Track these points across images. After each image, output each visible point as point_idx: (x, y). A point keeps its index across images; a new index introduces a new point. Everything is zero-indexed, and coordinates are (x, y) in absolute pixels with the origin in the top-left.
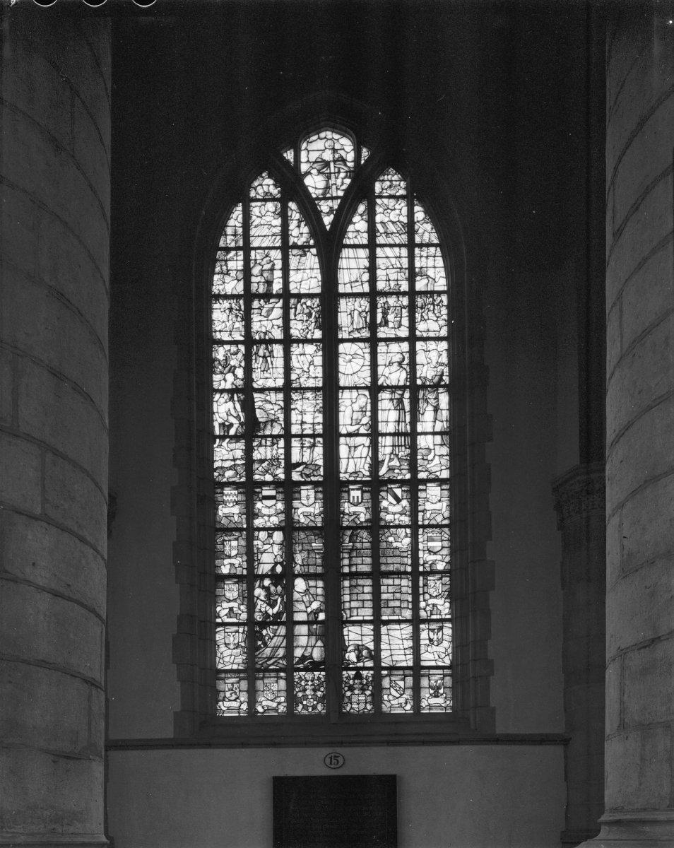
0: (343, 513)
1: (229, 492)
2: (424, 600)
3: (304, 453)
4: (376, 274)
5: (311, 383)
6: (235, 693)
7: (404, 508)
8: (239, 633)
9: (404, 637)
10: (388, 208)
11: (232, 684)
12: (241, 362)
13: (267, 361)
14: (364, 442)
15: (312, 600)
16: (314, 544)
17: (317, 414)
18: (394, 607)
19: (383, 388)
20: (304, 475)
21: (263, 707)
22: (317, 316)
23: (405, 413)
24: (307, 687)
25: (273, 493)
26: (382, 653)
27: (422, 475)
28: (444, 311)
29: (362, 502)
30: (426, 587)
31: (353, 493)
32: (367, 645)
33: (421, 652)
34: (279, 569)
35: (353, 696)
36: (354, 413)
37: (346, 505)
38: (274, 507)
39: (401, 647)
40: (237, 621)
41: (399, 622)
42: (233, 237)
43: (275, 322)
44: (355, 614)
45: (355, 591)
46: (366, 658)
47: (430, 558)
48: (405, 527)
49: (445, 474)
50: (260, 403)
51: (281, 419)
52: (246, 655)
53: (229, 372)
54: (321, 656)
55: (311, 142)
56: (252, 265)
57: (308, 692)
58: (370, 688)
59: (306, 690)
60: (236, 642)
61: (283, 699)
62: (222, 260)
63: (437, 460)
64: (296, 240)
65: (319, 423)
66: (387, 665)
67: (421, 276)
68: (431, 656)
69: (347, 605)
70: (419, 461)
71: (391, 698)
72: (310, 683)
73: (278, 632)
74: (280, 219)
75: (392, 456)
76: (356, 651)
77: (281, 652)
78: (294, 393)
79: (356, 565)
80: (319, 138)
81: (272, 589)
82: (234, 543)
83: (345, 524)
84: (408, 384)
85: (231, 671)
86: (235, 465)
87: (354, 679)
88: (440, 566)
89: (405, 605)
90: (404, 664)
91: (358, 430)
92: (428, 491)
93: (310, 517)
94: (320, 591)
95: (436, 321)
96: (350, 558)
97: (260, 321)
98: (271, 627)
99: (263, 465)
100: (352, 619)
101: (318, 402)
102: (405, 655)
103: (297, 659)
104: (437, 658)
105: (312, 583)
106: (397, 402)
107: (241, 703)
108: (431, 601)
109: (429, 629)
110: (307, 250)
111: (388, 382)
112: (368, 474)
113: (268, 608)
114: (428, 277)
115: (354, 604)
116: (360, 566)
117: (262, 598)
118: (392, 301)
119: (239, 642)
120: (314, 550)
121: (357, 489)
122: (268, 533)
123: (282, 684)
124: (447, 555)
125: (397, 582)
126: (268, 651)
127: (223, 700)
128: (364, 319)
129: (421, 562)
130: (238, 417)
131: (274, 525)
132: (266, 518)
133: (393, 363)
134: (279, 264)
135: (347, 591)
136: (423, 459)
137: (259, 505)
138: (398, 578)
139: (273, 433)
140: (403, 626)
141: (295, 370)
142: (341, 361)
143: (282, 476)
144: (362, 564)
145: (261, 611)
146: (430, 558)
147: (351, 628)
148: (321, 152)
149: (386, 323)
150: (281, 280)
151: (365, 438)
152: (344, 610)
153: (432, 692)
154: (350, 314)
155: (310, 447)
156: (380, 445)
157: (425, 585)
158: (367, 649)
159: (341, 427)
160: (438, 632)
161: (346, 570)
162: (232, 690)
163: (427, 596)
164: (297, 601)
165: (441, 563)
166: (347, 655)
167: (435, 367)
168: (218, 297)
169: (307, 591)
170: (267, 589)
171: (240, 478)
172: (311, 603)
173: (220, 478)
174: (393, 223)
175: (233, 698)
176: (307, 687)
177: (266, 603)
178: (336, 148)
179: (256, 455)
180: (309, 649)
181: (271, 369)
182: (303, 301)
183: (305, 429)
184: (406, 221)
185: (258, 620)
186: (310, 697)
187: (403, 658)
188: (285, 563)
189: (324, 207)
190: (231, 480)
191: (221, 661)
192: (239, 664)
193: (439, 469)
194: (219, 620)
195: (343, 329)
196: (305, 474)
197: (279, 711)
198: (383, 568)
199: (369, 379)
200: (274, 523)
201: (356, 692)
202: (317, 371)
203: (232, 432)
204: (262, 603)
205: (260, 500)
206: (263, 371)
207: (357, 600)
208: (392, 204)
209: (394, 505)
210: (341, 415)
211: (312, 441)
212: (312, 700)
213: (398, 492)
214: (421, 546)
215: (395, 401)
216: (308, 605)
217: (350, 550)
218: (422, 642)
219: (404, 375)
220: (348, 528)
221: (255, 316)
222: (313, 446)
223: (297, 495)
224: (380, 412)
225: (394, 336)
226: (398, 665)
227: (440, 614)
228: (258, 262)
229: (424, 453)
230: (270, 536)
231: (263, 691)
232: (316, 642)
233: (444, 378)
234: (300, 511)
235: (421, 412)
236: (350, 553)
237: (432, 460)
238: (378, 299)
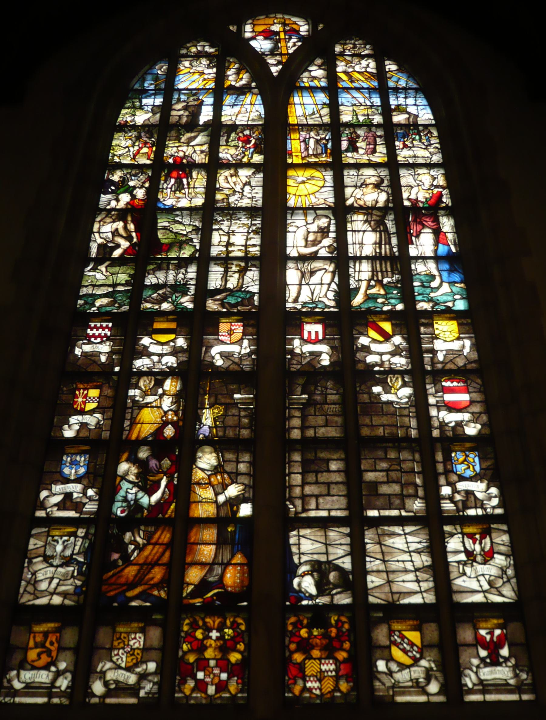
0: (292, 352)
1: (98, 325)
2: (449, 484)
3: (228, 278)
4: (338, 109)
5: (245, 203)
6: (49, 652)
7: (397, 347)
8: (76, 536)
9: (413, 547)
10: (352, 63)
11: (46, 634)
12: (144, 183)
13: (182, 182)
14: (326, 267)
15: (228, 481)
16: (237, 396)
17: (251, 235)
18: (389, 495)
19: (354, 210)
20: (227, 305)
21: (106, 684)
22: (258, 142)
23: (389, 234)
24: (208, 642)
25: (173, 326)
26: (369, 578)
27: (423, 306)
28: (434, 141)
29: (324, 338)
30: (449, 463)
31: (308, 328)
32: (338, 562)
33: (452, 576)
34: (169, 432)
35: (308, 663)
36: (311, 234)
37: (297, 342)
38: (172, 344)
39: (409, 566)
40: (77, 515)
41: (400, 521)
42: (153, 82)
43: (198, 148)
44: (313, 505)
45: (314, 467)
46: (336, 587)
47: (451, 418)
48: (402, 373)
49: (461, 305)
50: (166, 224)
51: (195, 240)
52: (83, 578)
53: (125, 192)
54: (242, 581)
55: (258, 20)
56: (173, 102)
57: (209, 653)
58: (347, 645)
59: (205, 648)
60: (68, 553)
61: (152, 666)
62: (136, 98)
63: (446, 288)
64: (233, 83)
65: (254, 246)
66: (379, 601)
67: (399, 111)
68: (474, 585)
69: (297, 491)
70: (416, 289)
71: (394, 667)
72: (214, 634)
73: (157, 536)
74: (215, 70)
75: (373, 283)
76: (315, 574)
77: (157, 574)
78: (217, 214)
79: (315, 427)
80: (267, 17)
81: (153, 463)
82: (94, 393)
83: (295, 367)
84: (391, 205)
85: (49, 607)
86: (114, 292)
87: (310, 627)
88: (472, 430)
89: (411, 491)
90: (417, 599)
91: (317, 252)
92: (436, 326)
93: (232, 358)
94: (242, 467)
95: (424, 149)
96: (304, 418)
97: (177, 147)
98: (142, 528)
99: (160, 292)
100: (304, 515)
101: (253, 222)
102: (418, 581)
103: (191, 588)
104: (486, 586)
105: (229, 456)
106: (375, 224)
107: (58, 674)
108: (462, 486)
109: (463, 534)
110: (246, 90)
111: (361, 203)
112: (332, 303)
113: (140, 494)
114: (409, 113)
115: (308, 490)
116: (322, 430)
117: (132, 478)
118: (361, 132)
119: (73, 554)
120: (237, 403)
121: (316, 323)
122: (156, 380)
123: (155, 634)
124: (480, 413)
125: (392, 455)
126: (131, 571)
127: (23, 665)
128: (323, 145)
129: (436, 424)
130: (129, 238)
131: (168, 367)
132: (155, 358)
133: (366, 185)
134: (209, 100)
135: (298, 468)
136: (423, 286)
137: (146, 341)
138: (394, 447)
139: (182, 256)
140: (408, 529)
141: (223, 190)
142: (290, 182)
143: (190, 306)
144: (326, 425)
145: (125, 499)
146: (451, 418)
147: (303, 532)
148: (269, 26)
149: (353, 147)
150: (212, 114)
151: (328, 262)
152: (291, 499)
153: (483, 653)
154: (304, 141)
155: (239, 272)
156: (351, 270)
157: (448, 459)
158: (338, 568)
159: (288, 251)
160: (483, 537)
161: (296, 434)
162: (43, 645)
163: (454, 478)
164: (199, 484)
165: (473, 425)
166: (296, 581)
167: (429, 189)
168: (125, 128)
169: (217, 470)
170: (142, 465)
171: (120, 306)
172: (225, 487)
173: (87, 307)
174: (359, 72)
175: (41, 663)
176: (208, 642)
177: (138, 486)
178: (287, 22)
179: (150, 280)
180: (218, 570)
181: (187, 190)
182: (238, 130)
183: (233, 251)
184: (374, 71)
185: (119, 513)
186: (212, 663)
187: (414, 586)
188: (181, 424)
189: (271, 61)
190: (103, 310)
191: (30, 589)
192: (65, 595)
193: (450, 298)
194: (41, 514)
195: (294, 154)
196: (229, 303)
197: (142, 693)
198: (365, 432)
199: (332, 200)
200: (169, 364)
201: (316, 653)
202: (254, 191)
203: (117, 253)
204: (130, 486)
205: (150, 335)
206: (175, 192)
207: (317, 483)
208: (357, 60)
209: (380, 342)
210: (289, 236)
211: (243, 264)
212: (216, 671)
213: (387, 326)
214: (432, 400)
215: (373, 223)
216: (219, 490)
217: (303, 404)
218: (451, 558)
219: (382, 198)
220: (299, 373)
221: (171, 142)
222: (243, 272)
223: (211, 330)
224: (349, 234)
225: (367, 162)
226: (406, 601)
227: (482, 507)
228: (182, 100)
229: (424, 279)
230: (159, 383)
231: (112, 649)
232: (233, 556)
233: (444, 200)
234: (215, 350)
235: (414, 234)
236: (302, 410)
237: (438, 288)
238: (341, 129)
